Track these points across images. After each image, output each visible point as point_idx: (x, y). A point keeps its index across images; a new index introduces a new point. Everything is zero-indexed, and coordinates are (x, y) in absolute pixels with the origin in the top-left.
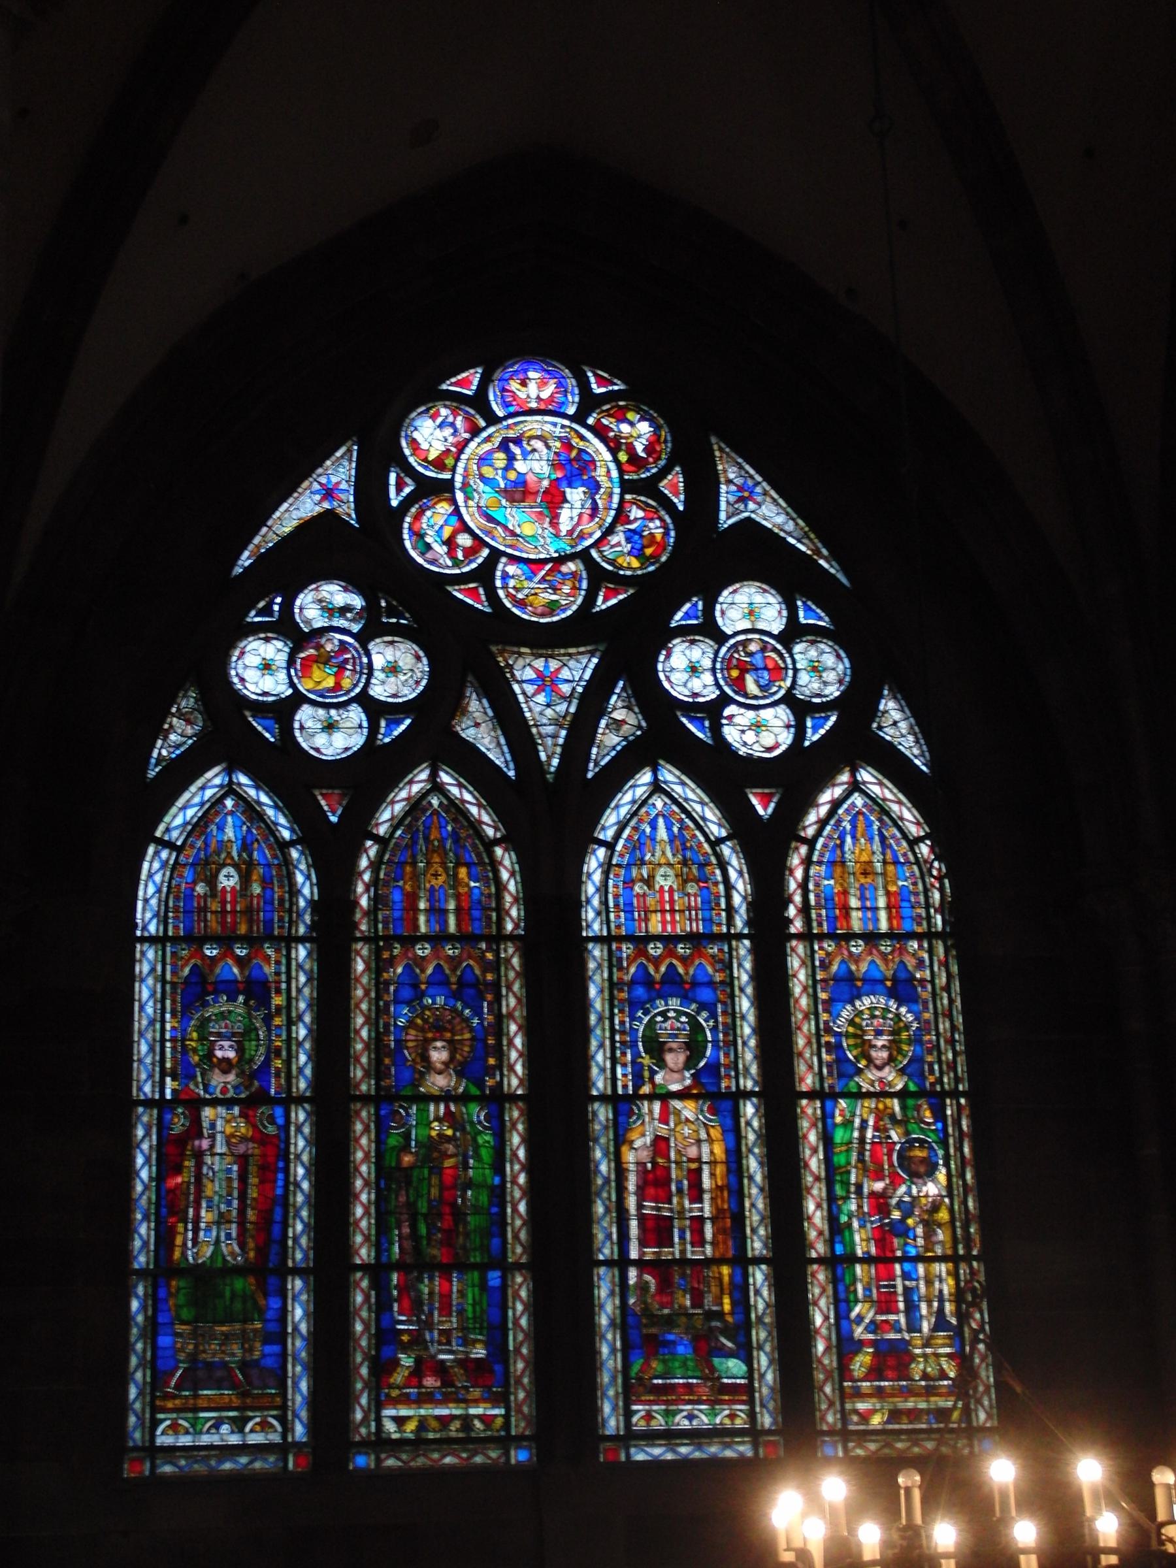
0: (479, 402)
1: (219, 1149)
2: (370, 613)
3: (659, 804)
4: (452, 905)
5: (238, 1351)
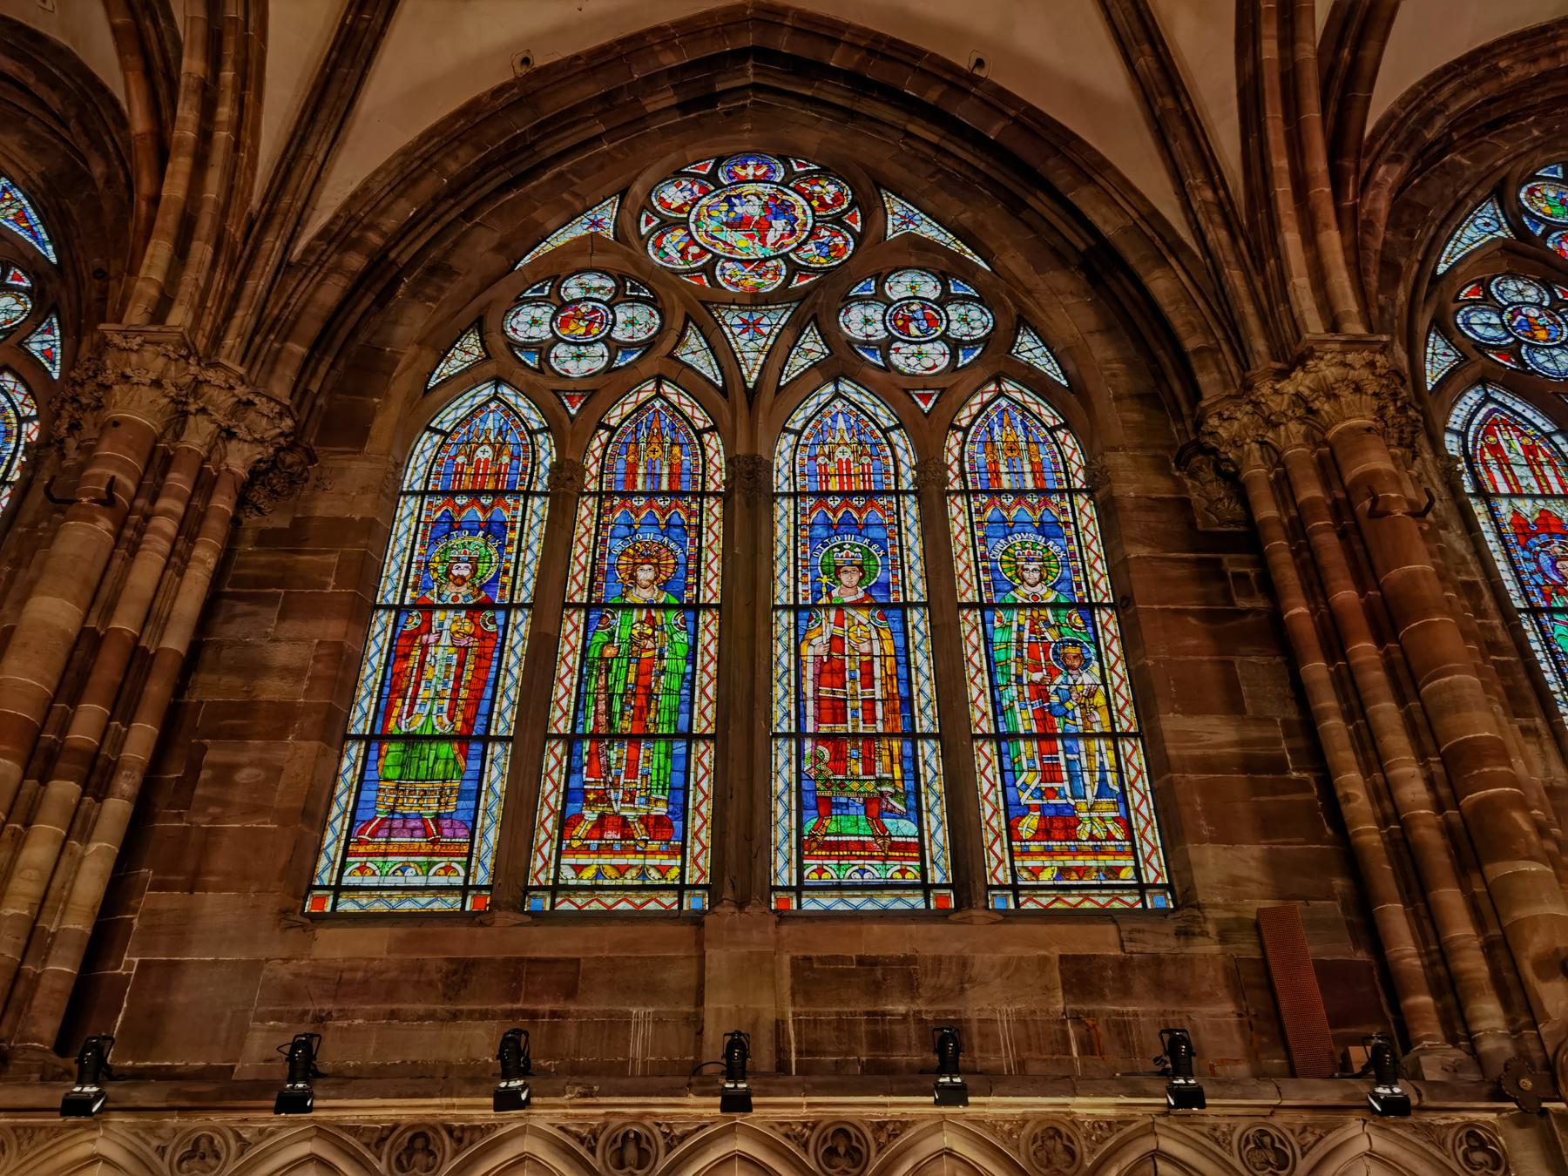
0: (712, 177)
1: (446, 640)
2: (619, 288)
3: (839, 405)
4: (666, 470)
5: (434, 806)
